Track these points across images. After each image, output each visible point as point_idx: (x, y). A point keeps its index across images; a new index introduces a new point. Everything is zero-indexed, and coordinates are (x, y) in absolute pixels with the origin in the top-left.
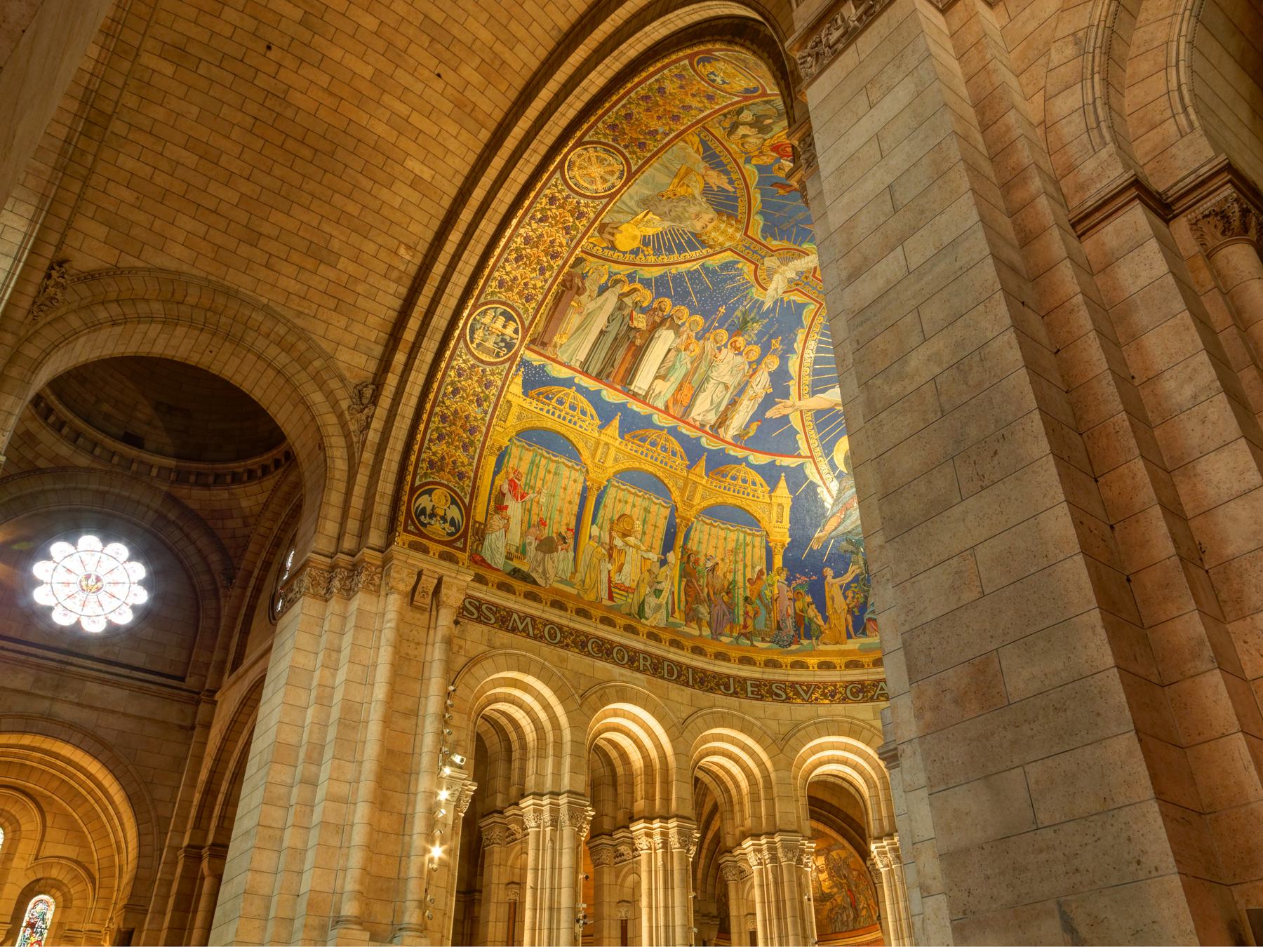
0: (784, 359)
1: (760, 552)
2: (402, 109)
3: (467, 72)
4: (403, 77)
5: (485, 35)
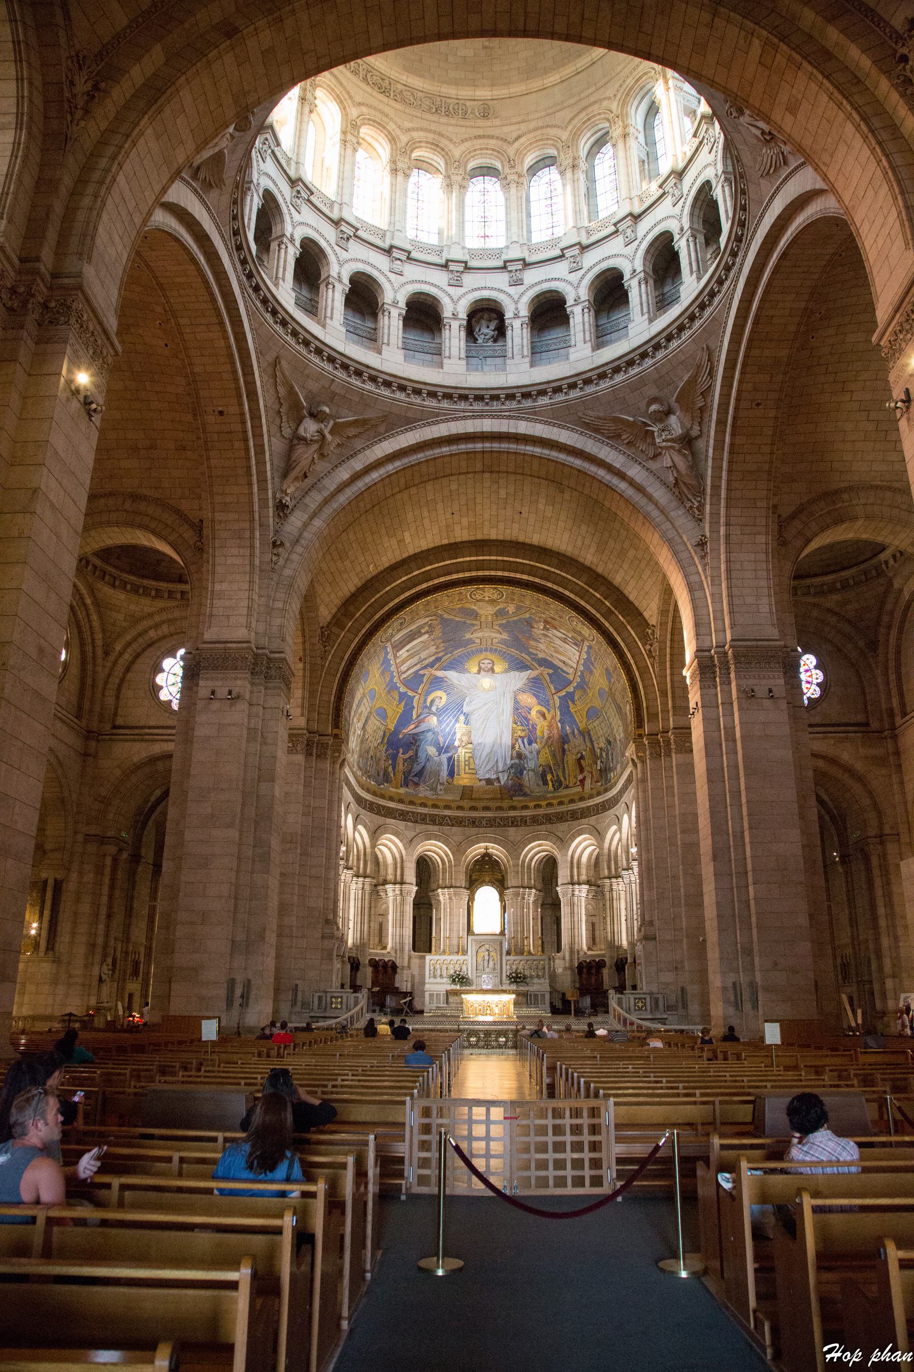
0: (446, 654)
1: (381, 733)
2: (426, 514)
3: (465, 521)
4: (440, 506)
5: (486, 516)
